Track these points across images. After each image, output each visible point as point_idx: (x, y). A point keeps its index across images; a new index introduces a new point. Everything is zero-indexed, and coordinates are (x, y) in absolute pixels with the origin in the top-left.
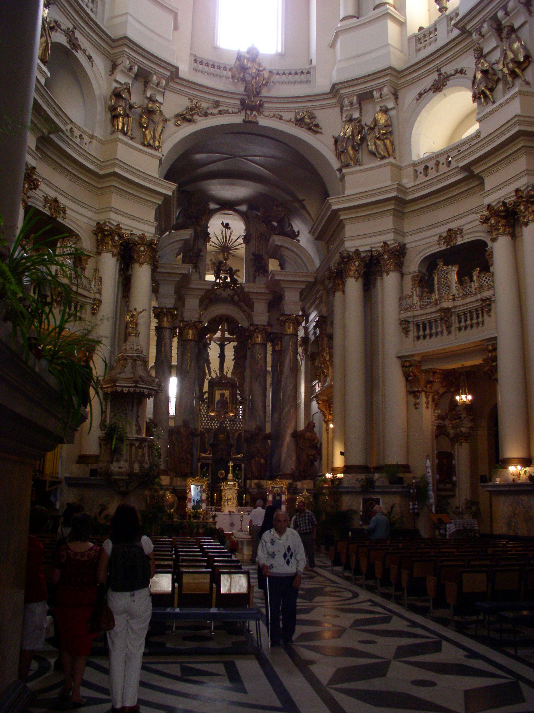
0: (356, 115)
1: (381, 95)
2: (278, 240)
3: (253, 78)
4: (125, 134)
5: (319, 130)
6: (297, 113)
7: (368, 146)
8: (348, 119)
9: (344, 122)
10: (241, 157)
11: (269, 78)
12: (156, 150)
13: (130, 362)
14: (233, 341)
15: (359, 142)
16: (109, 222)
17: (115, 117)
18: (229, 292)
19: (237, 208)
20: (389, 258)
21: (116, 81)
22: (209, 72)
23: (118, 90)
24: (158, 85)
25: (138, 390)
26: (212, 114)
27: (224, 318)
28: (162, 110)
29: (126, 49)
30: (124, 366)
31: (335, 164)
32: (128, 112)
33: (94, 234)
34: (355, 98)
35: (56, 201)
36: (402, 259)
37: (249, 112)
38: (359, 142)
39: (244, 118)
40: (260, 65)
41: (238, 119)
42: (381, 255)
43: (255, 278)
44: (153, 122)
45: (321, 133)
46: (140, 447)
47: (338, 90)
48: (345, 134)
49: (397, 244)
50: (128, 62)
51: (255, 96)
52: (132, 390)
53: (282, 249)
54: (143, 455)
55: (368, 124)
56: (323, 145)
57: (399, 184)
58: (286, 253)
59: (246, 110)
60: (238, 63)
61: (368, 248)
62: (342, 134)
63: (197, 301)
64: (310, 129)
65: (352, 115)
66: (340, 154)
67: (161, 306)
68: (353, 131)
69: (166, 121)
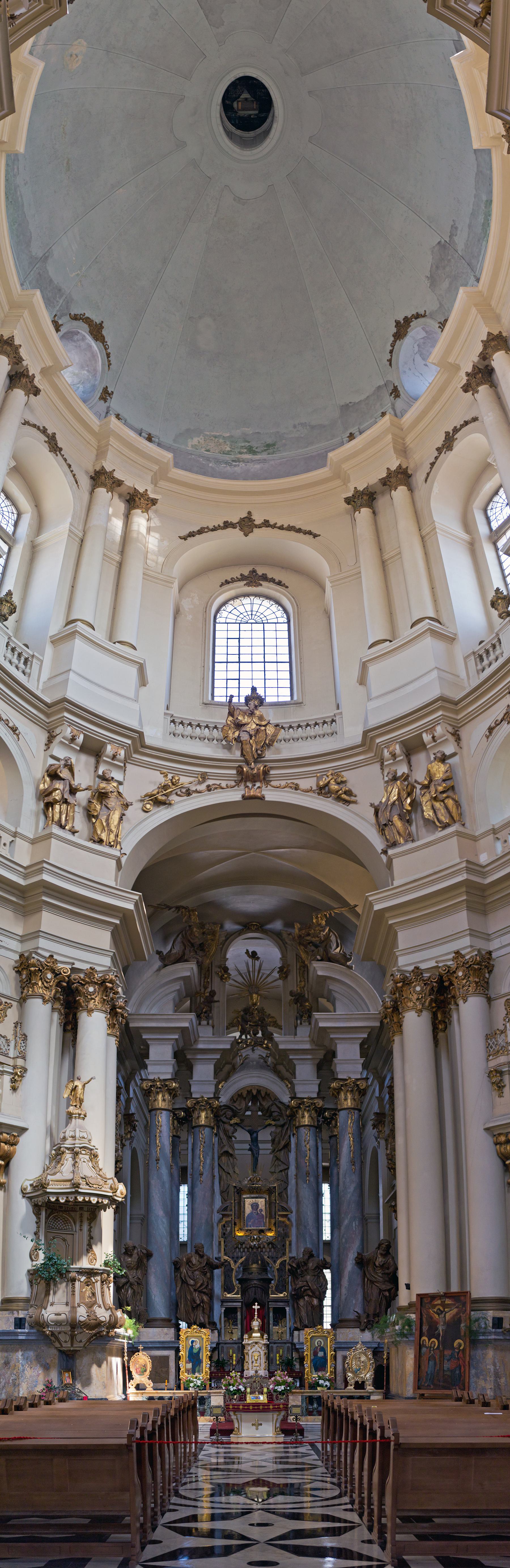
0: (402, 769)
1: (433, 737)
2: (320, 969)
3: (251, 736)
4: (63, 827)
5: (353, 799)
6: (319, 779)
7: (423, 811)
8: (390, 776)
9: (386, 782)
10: (257, 851)
11: (275, 735)
12: (111, 846)
14: (270, 1125)
15: (409, 808)
16: (37, 954)
17: (49, 805)
18: (260, 1052)
19: (269, 926)
20: (466, 976)
21: (53, 757)
22: (193, 735)
23: (53, 768)
24: (114, 757)
26: (197, 791)
27: (255, 1092)
28: (121, 791)
29: (66, 714)
31: (378, 844)
32: (66, 797)
33: (17, 972)
34: (397, 747)
36: (487, 975)
37: (250, 785)
38: (409, 808)
39: (243, 792)
40: (261, 718)
41: (235, 795)
43: (296, 1028)
44: (108, 808)
45: (355, 802)
47: (373, 739)
48: (388, 799)
49: (476, 953)
50: (69, 730)
51: (256, 761)
53: (328, 982)
55: (420, 780)
56: (359, 819)
57: (468, 862)
59: (246, 782)
60: (230, 718)
61: (432, 964)
62: (384, 800)
63: (212, 1067)
64: (339, 799)
65: (396, 772)
66: (383, 828)
67: (151, 1077)
68: (399, 794)
69: (126, 806)
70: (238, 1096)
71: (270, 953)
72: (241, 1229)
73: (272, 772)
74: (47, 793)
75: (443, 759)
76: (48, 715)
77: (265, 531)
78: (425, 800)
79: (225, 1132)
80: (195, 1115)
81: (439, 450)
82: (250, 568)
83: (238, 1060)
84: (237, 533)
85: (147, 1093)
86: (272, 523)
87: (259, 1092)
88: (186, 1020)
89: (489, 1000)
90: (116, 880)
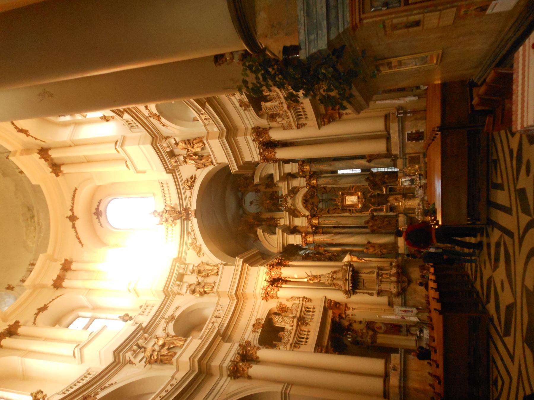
2: (257, 180)
4: (214, 287)
13: (335, 281)
17: (205, 293)
18: (289, 199)
19: (240, 197)
24: (184, 269)
25: (350, 278)
26: (194, 236)
29: (169, 289)
30: (338, 285)
35: (254, 325)
40: (163, 212)
42: (260, 143)
46: (382, 276)
52: (350, 282)
54: (386, 274)
58: (263, 175)
69: (202, 263)
70: (306, 207)
71: (250, 197)
72: (358, 205)
73: (185, 207)
74: (201, 294)
75: (177, 144)
76: (170, 296)
77: (75, 211)
78: (194, 151)
79: (320, 212)
80: (314, 224)
81: (28, 135)
82: (93, 215)
83: (292, 208)
84: (78, 223)
85: (307, 244)
86: (71, 208)
87: (304, 200)
88: (279, 231)
89: (270, 128)
90: (232, 265)
